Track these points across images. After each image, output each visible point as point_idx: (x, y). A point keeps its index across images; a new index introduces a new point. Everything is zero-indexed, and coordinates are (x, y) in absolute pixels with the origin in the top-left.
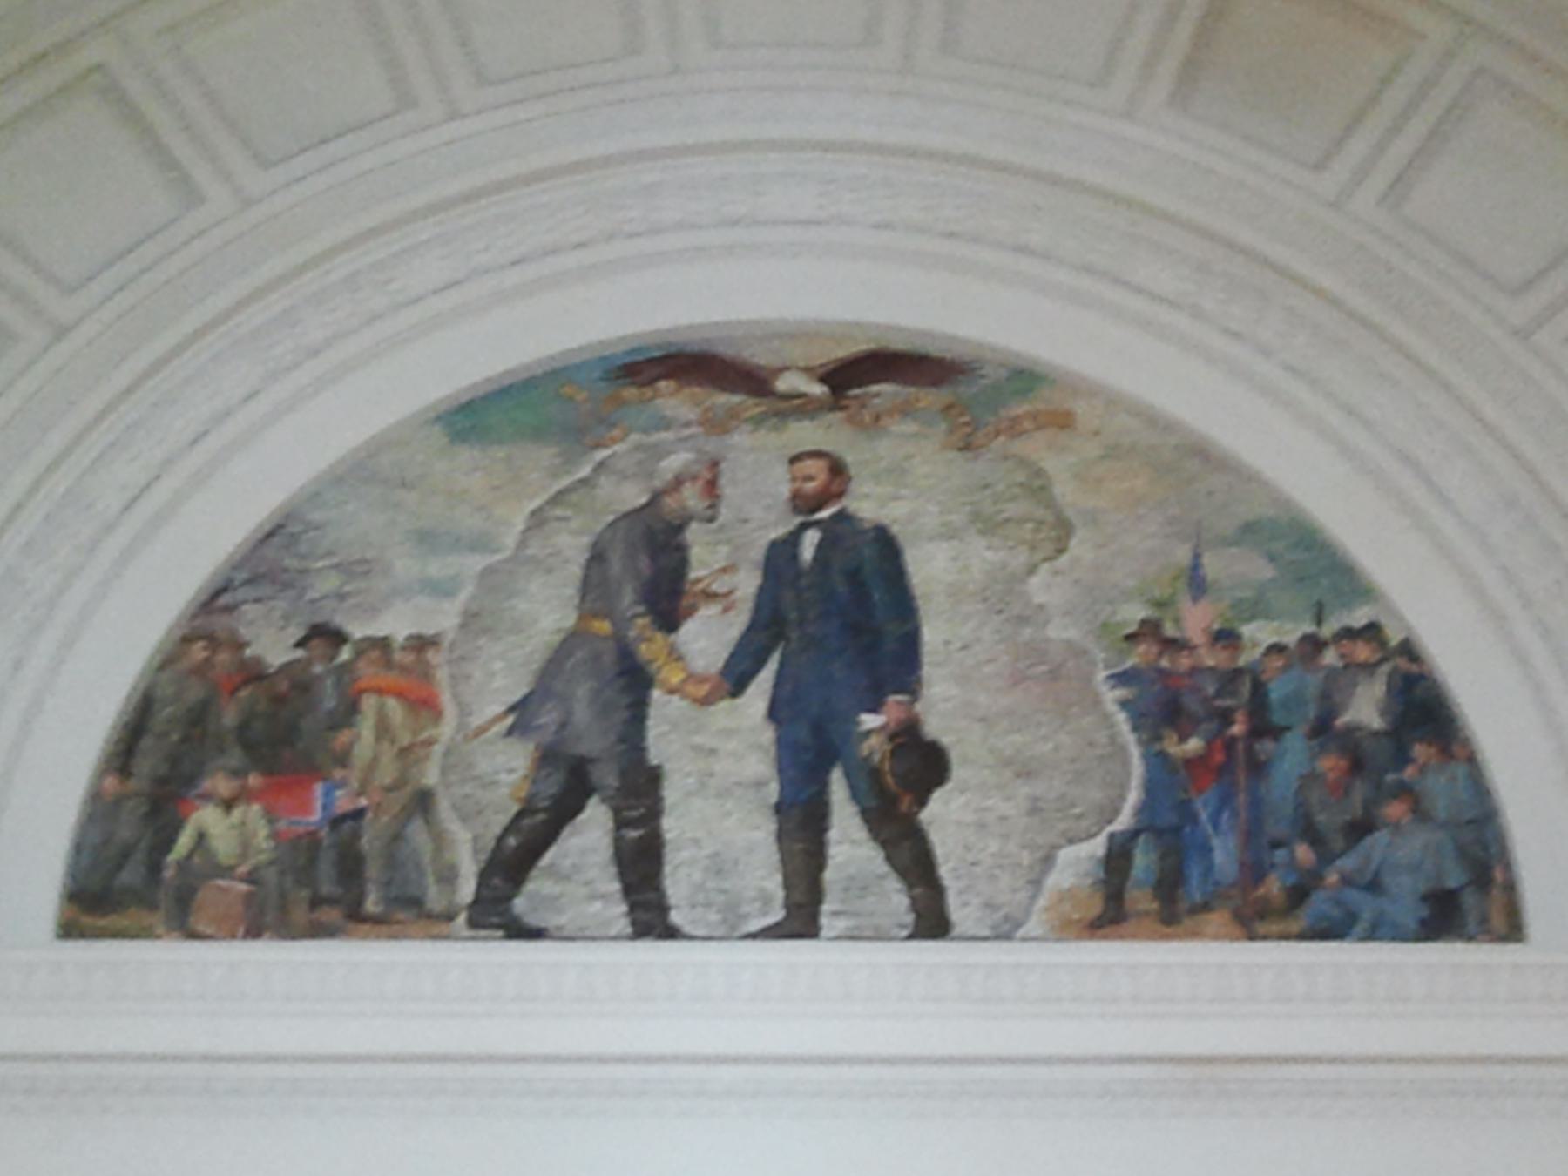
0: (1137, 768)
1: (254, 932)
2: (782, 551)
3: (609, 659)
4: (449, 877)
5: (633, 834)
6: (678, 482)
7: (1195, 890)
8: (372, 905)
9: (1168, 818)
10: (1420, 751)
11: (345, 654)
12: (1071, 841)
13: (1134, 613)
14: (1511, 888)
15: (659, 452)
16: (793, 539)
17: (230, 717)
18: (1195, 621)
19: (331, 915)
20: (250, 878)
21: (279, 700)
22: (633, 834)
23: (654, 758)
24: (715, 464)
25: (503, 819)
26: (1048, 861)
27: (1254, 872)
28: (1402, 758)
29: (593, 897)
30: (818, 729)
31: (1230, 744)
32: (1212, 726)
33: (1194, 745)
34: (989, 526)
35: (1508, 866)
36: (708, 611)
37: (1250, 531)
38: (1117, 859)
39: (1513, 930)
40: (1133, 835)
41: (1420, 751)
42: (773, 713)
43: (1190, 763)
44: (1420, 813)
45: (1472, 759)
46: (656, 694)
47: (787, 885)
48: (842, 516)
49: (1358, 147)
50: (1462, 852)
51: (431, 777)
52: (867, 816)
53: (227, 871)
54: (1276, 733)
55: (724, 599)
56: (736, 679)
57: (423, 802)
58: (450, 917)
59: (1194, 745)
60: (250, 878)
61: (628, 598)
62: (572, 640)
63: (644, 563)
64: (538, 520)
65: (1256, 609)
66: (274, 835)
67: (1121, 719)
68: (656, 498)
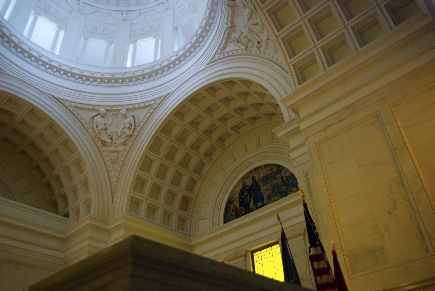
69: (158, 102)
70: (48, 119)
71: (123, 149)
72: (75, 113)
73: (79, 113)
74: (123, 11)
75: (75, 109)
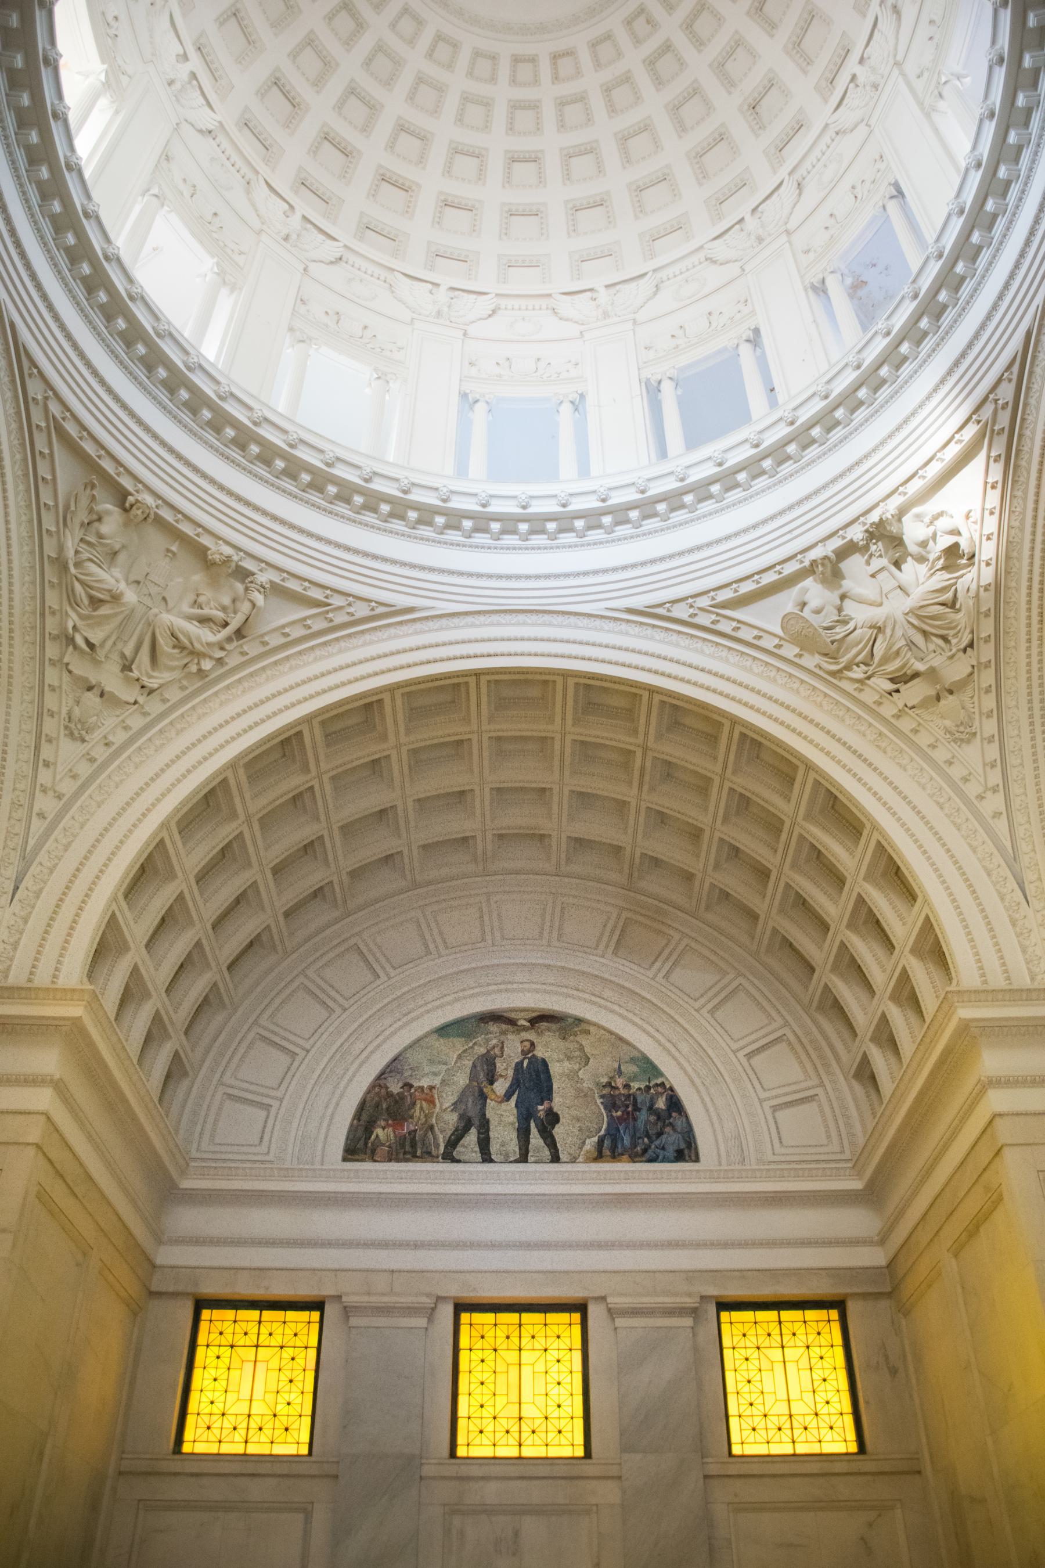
0: (606, 1119)
1: (390, 1160)
2: (519, 1065)
3: (476, 1094)
4: (437, 1146)
5: (482, 1136)
6: (494, 1047)
7: (620, 1150)
8: (419, 1153)
9: (614, 1132)
10: (674, 1114)
11: (413, 1090)
12: (589, 1137)
13: (604, 1080)
14: (696, 1148)
15: (488, 1040)
16: (522, 1062)
17: (384, 1106)
18: (620, 1082)
19: (408, 1156)
20: (389, 1147)
21: (396, 1102)
22: (482, 1136)
23: (488, 1116)
24: (503, 1043)
25: (449, 1133)
26: (584, 1143)
27: (634, 1145)
28: (670, 1116)
29: (473, 1151)
30: (528, 1110)
31: (628, 1113)
32: (623, 1109)
33: (619, 1113)
34: (569, 1058)
35: (695, 1144)
36: (501, 1080)
37: (633, 1060)
38: (601, 1142)
39: (697, 1160)
40: (605, 1136)
41: (674, 1114)
42: (516, 1106)
43: (618, 1118)
44: (674, 1130)
45: (687, 1117)
46: (488, 1101)
47: (520, 1149)
48: (534, 1055)
49: (658, 964)
50: (684, 1138)
51: (434, 1121)
52: (539, 1131)
53: (383, 1145)
54: (638, 1110)
55: (505, 1077)
56: (508, 1096)
57: (431, 1128)
58: (438, 1157)
59: (619, 1113)
60: (389, 1147)
61: (481, 1076)
62: (468, 1086)
63: (485, 1067)
64: (460, 1057)
65: (634, 1078)
66: (395, 1136)
67: (602, 1107)
68: (488, 1051)
69: (1006, 392)
70: (646, 695)
71: (973, 667)
72: (725, 627)
73: (739, 622)
74: (742, 220)
75: (718, 614)
